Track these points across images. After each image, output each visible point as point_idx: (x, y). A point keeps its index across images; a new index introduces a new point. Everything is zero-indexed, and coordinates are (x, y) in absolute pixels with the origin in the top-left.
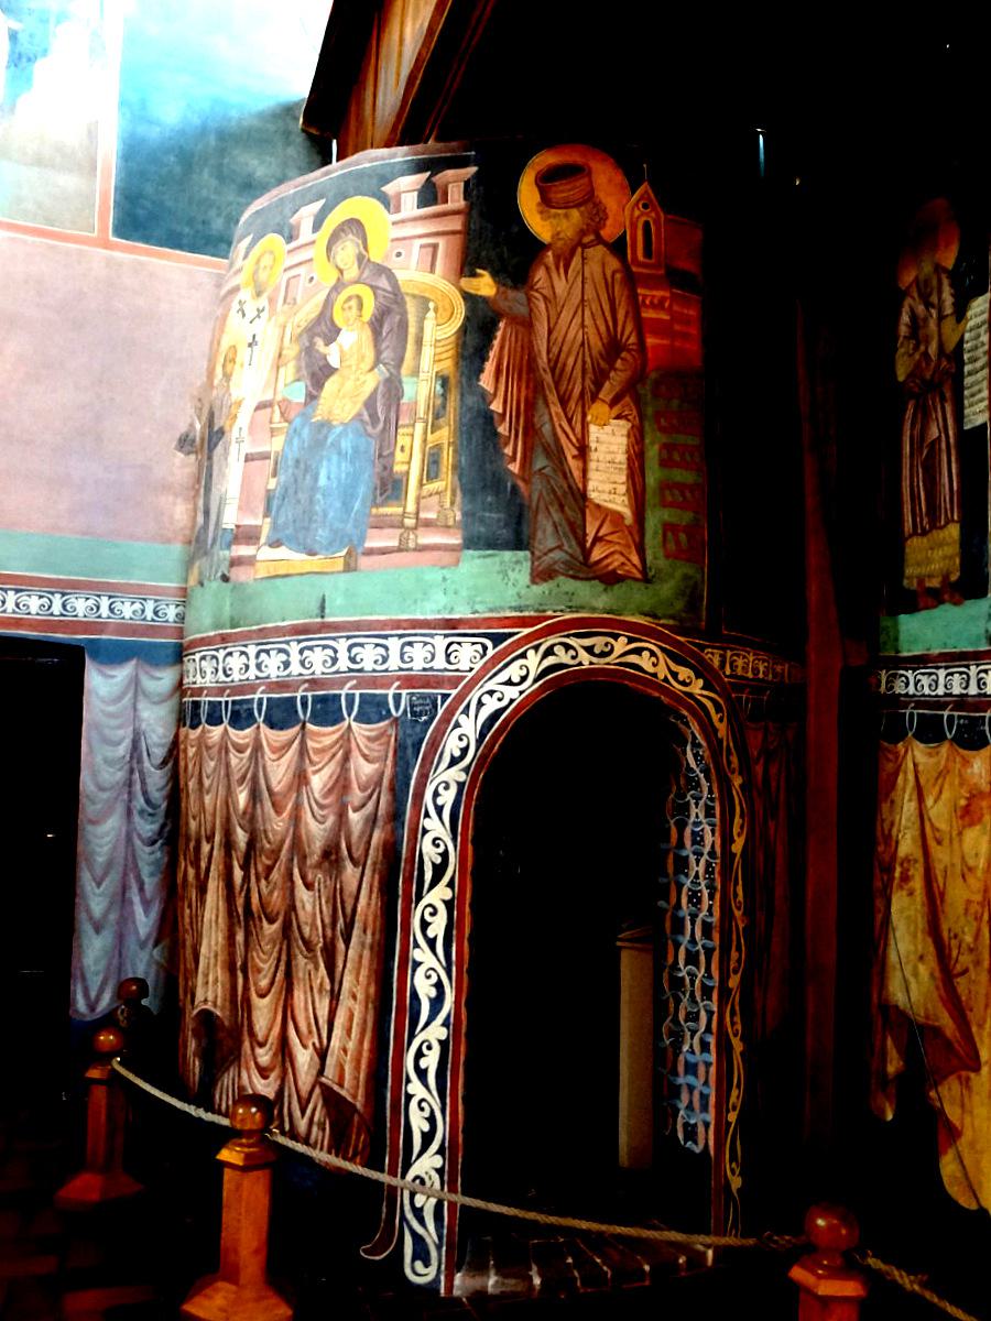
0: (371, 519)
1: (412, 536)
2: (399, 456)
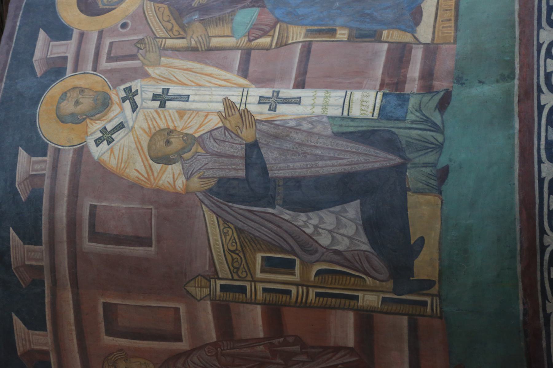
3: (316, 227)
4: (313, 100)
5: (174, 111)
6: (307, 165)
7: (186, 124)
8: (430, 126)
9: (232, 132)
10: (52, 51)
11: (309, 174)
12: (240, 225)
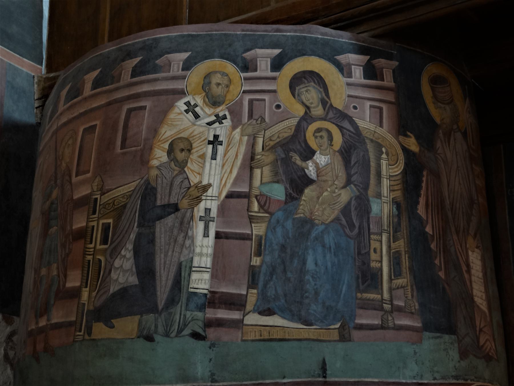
0: (358, 301)
1: (390, 318)
2: (374, 256)
3: (124, 256)
4: (206, 246)
5: (205, 151)
6: (162, 246)
7: (194, 161)
8: (181, 328)
9: (186, 193)
10: (262, 60)
11: (156, 248)
12: (128, 206)
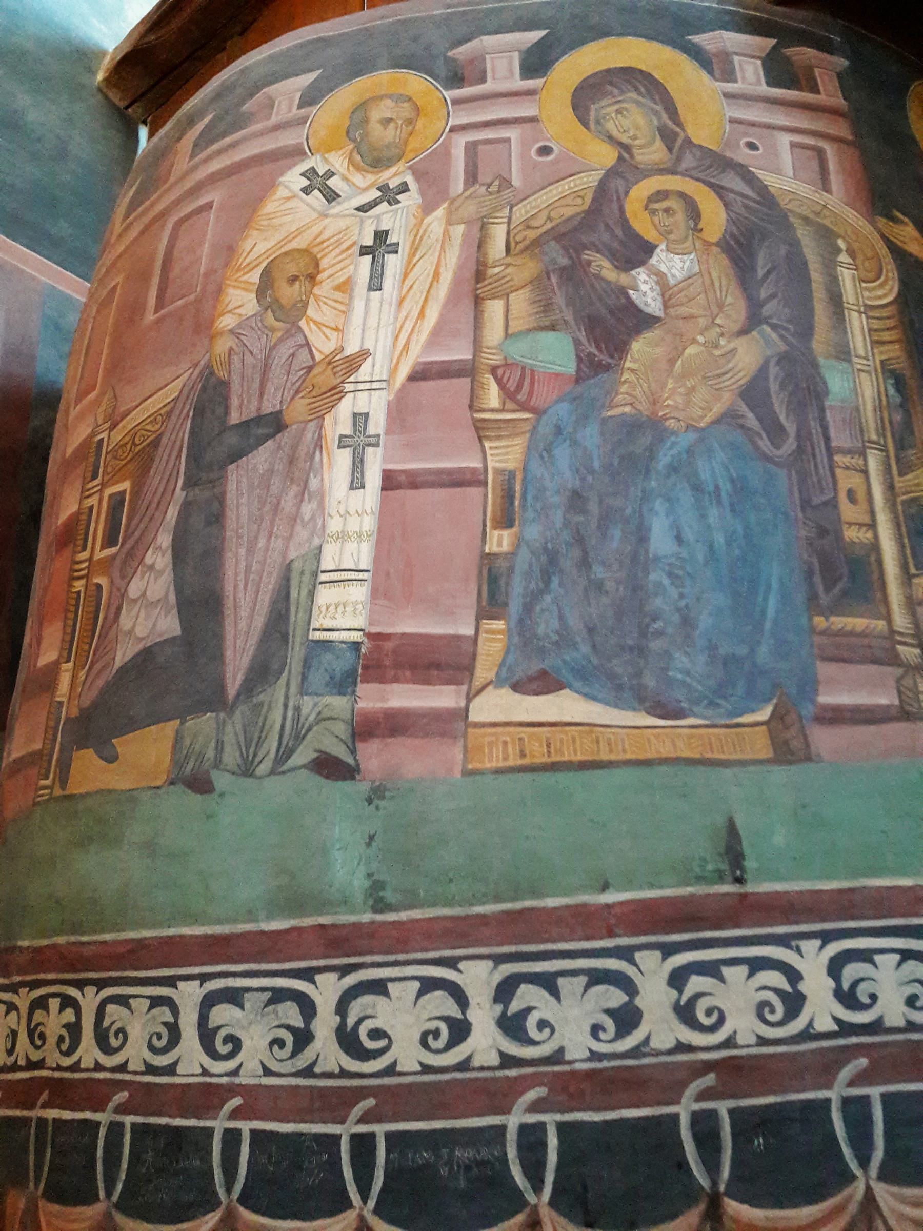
0: (817, 639)
2: (848, 511)
3: (151, 568)
4: (357, 512)
12: (164, 440)
